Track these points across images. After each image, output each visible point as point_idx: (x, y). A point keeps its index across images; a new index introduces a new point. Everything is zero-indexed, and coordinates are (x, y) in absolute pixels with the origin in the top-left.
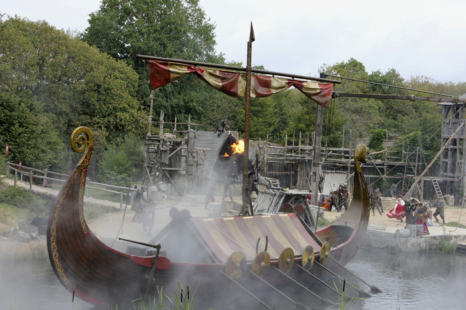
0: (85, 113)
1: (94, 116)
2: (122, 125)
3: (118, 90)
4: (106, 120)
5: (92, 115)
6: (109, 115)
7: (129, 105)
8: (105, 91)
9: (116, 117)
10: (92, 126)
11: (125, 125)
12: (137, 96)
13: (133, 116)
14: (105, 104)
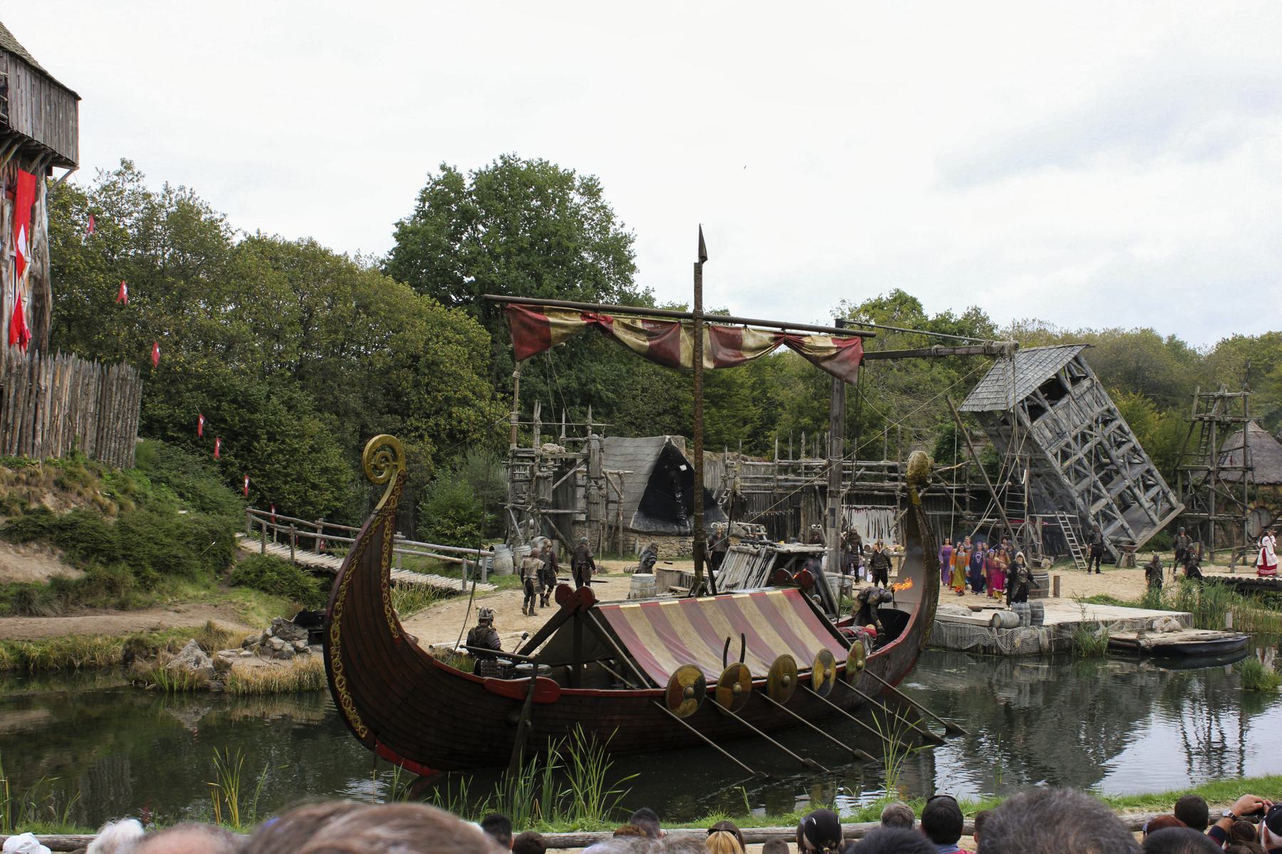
0: (392, 411)
1: (409, 416)
2: (461, 432)
3: (452, 365)
4: (432, 422)
5: (404, 413)
6: (437, 413)
7: (474, 393)
8: (429, 367)
9: (450, 415)
10: (406, 436)
11: (468, 431)
12: (489, 375)
13: (482, 413)
14: (428, 393)
